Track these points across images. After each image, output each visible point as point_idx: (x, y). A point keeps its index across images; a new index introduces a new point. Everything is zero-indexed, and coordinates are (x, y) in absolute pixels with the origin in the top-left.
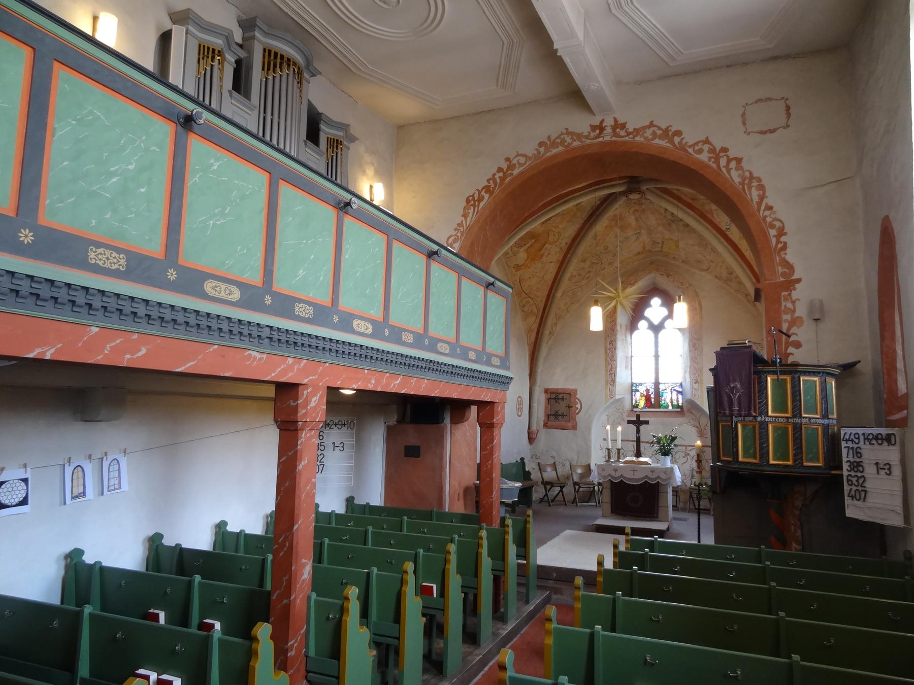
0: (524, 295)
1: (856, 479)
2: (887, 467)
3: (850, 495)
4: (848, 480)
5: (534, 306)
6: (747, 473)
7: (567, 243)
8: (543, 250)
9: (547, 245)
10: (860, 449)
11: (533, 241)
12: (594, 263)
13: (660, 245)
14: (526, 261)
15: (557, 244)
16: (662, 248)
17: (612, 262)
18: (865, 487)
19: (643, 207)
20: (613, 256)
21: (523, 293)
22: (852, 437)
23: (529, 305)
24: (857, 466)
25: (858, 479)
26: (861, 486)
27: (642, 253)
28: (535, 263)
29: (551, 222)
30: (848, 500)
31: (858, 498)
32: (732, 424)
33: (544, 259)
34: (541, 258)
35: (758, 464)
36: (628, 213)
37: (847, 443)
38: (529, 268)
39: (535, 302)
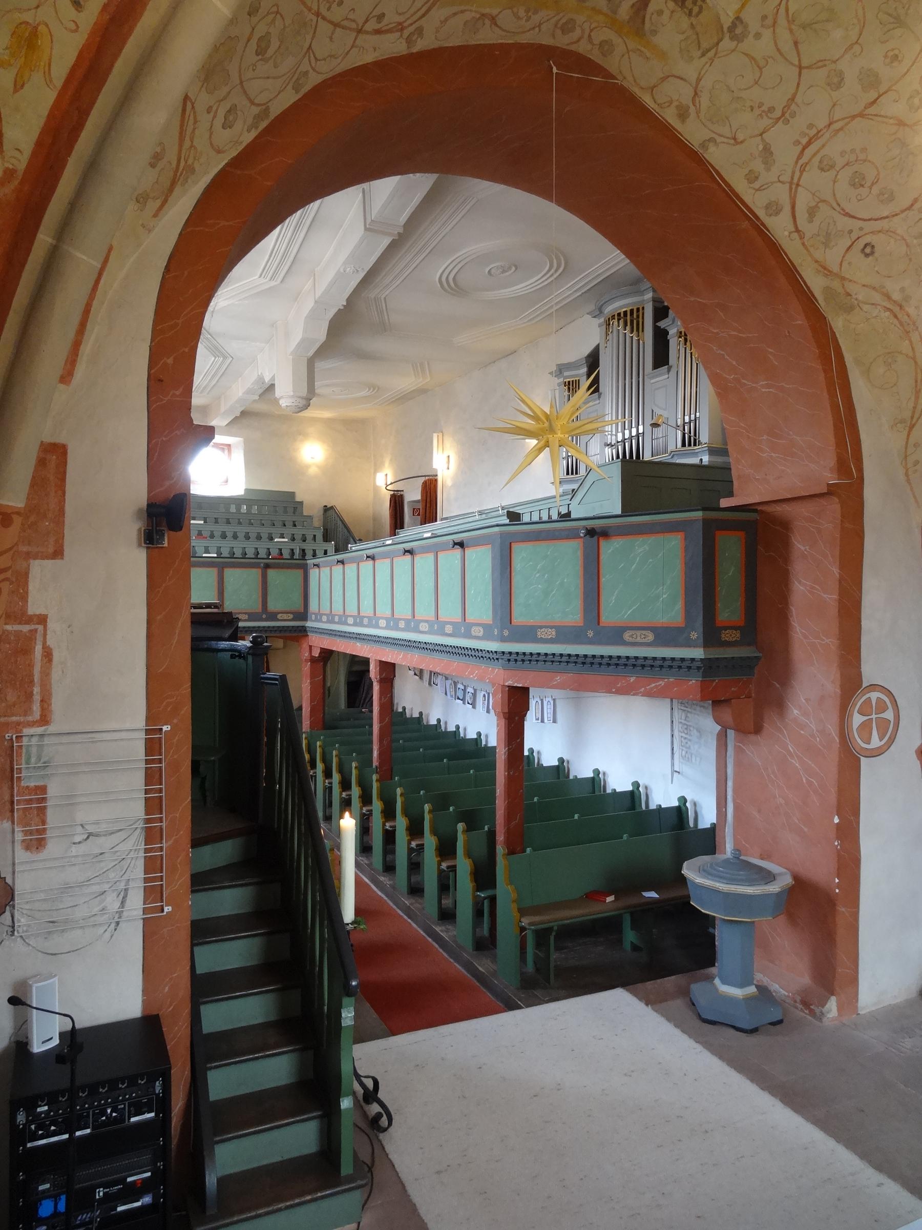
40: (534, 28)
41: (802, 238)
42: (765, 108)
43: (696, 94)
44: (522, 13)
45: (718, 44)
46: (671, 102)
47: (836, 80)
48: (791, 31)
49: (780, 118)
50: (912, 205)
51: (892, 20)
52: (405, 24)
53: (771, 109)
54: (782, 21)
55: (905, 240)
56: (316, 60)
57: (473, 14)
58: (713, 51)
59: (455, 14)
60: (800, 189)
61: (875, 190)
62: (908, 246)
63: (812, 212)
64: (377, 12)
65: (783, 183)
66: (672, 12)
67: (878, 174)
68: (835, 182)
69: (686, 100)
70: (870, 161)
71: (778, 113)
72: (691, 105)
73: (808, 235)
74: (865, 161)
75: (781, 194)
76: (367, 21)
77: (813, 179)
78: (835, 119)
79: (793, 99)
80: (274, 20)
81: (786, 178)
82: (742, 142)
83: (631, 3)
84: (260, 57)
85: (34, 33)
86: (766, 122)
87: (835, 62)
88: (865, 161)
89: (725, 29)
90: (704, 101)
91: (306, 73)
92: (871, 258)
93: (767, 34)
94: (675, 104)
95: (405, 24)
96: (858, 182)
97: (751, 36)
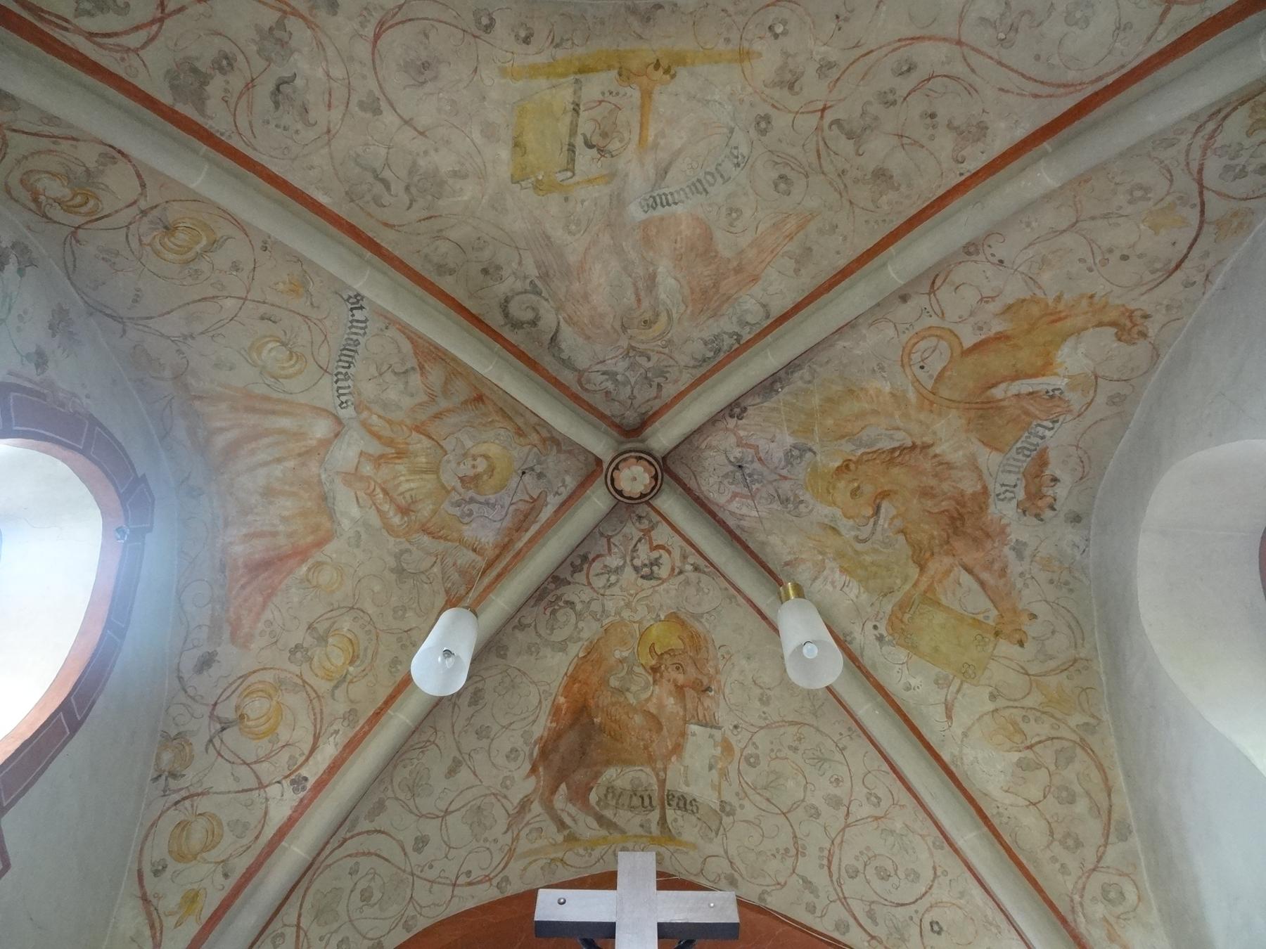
0: (1216, 207)
5: (1220, 140)
7: (904, 298)
8: (994, 331)
9: (968, 342)
11: (998, 392)
12: (850, 135)
13: (586, 127)
14: (1079, 331)
15: (934, 321)
16: (576, 111)
17: (781, 84)
19: (624, 343)
20: (767, 119)
21: (1209, 214)
23: (1241, 161)
27: (657, 66)
28: (1059, 299)
29: (900, 435)
33: (1015, 290)
34: (1024, 301)
36: (675, 316)
38: (1092, 297)
39: (1196, 154)
40: (599, 860)
41: (881, 942)
42: (782, 851)
43: (731, 863)
44: (581, 851)
45: (721, 823)
46: (719, 876)
47: (813, 811)
48: (759, 794)
49: (797, 853)
50: (935, 873)
51: (816, 761)
52: (491, 876)
53: (787, 850)
54: (750, 792)
55: (954, 904)
56: (421, 907)
57: (545, 861)
58: (722, 829)
59: (531, 863)
60: (849, 901)
61: (901, 874)
62: (960, 908)
63: (871, 915)
64: (464, 869)
65: (834, 901)
66: (683, 816)
67: (893, 862)
68: (869, 883)
69: (729, 871)
70: (879, 855)
71: (793, 851)
72: (733, 872)
73: (884, 938)
74: (875, 856)
75: (837, 911)
76: (457, 878)
77: (850, 887)
78: (833, 836)
79: (795, 837)
80: (373, 878)
81: (834, 897)
82: (785, 883)
83: (656, 823)
84: (365, 903)
85: (197, 894)
86: (789, 862)
87: (803, 801)
88: (875, 856)
89: (718, 810)
90: (741, 867)
91: (413, 917)
92: (943, 934)
93: (746, 803)
94: (722, 876)
95: (491, 876)
96: (884, 876)
97: (738, 809)
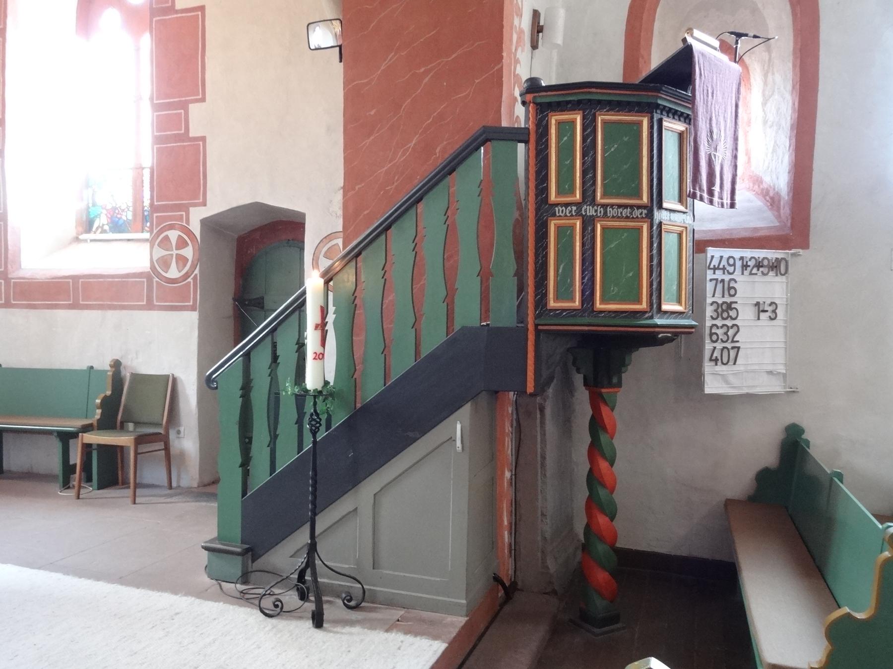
1: (725, 329)
2: (770, 309)
3: (714, 358)
4: (711, 334)
6: (669, 335)
10: (736, 282)
18: (738, 341)
22: (724, 262)
24: (726, 309)
25: (728, 331)
26: (733, 341)
30: (708, 367)
31: (725, 360)
32: (651, 226)
35: (684, 313)
37: (714, 273)
